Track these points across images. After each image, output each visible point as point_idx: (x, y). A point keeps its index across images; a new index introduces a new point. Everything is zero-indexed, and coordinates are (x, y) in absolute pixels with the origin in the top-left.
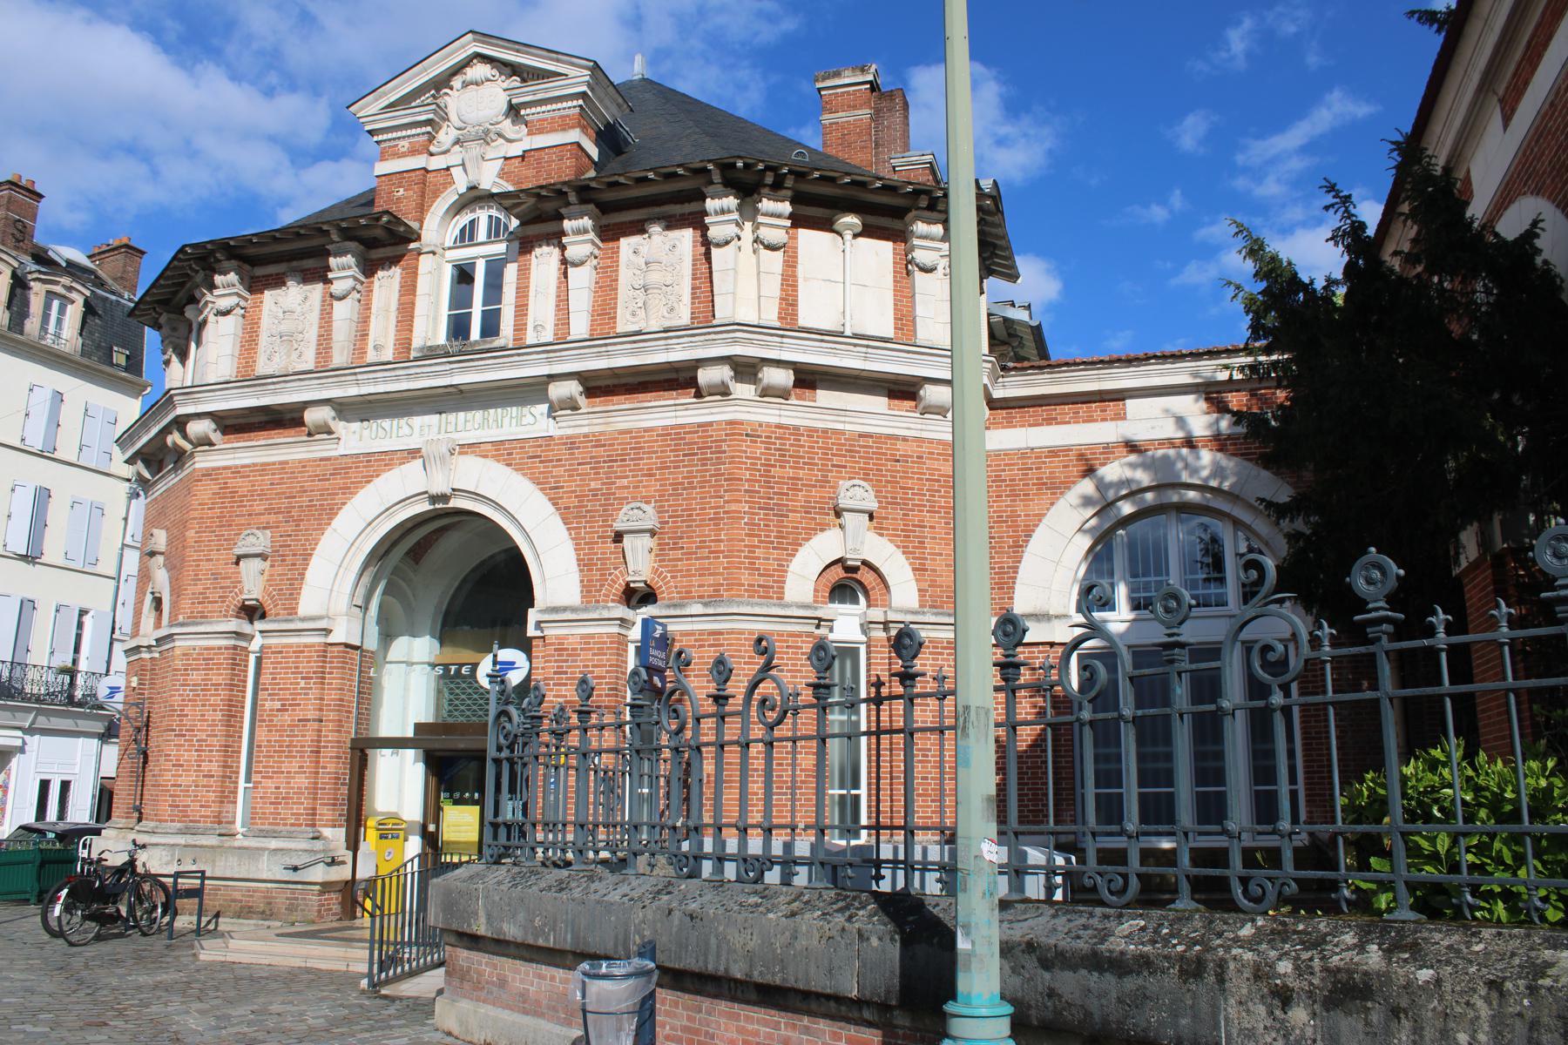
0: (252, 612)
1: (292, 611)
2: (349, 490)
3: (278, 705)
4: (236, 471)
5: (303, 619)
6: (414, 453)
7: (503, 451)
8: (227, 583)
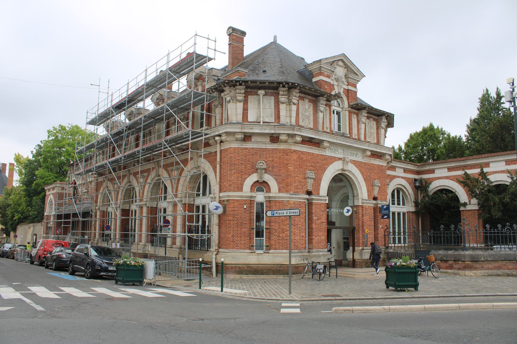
0: (309, 193)
1: (318, 194)
2: (328, 164)
3: (317, 218)
4: (302, 153)
5: (321, 197)
6: (340, 159)
7: (354, 162)
8: (303, 184)
